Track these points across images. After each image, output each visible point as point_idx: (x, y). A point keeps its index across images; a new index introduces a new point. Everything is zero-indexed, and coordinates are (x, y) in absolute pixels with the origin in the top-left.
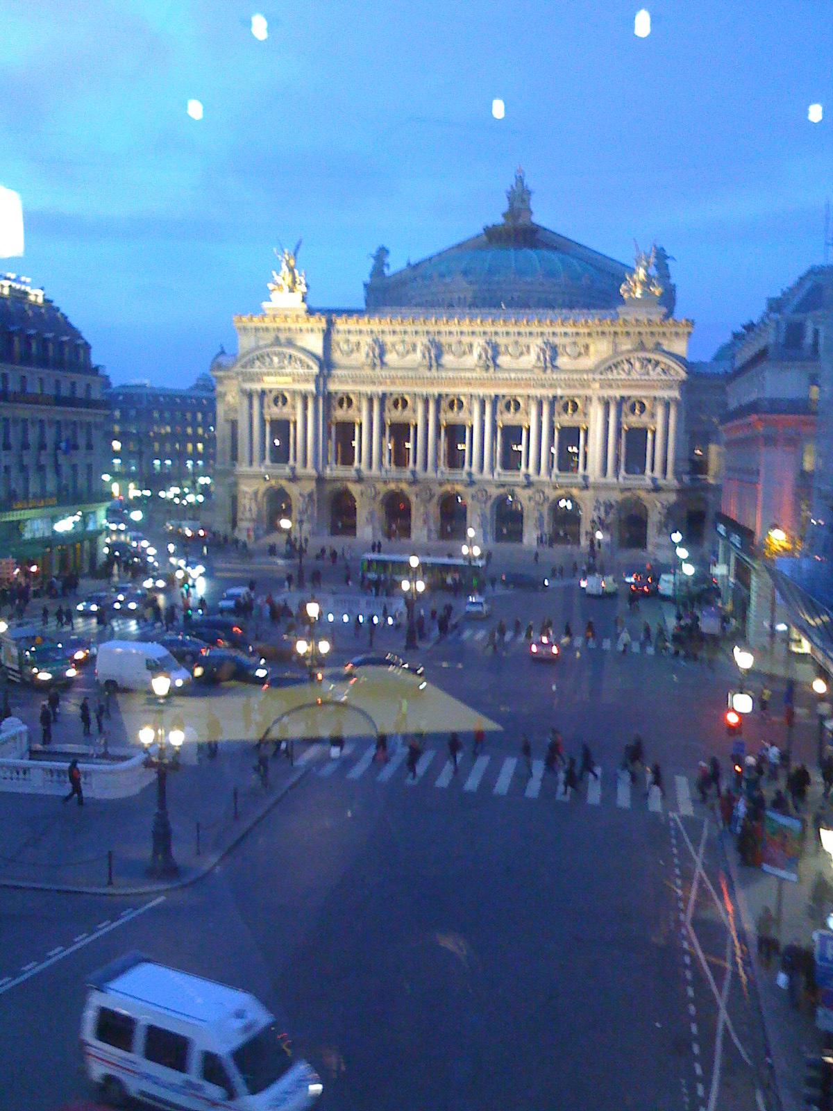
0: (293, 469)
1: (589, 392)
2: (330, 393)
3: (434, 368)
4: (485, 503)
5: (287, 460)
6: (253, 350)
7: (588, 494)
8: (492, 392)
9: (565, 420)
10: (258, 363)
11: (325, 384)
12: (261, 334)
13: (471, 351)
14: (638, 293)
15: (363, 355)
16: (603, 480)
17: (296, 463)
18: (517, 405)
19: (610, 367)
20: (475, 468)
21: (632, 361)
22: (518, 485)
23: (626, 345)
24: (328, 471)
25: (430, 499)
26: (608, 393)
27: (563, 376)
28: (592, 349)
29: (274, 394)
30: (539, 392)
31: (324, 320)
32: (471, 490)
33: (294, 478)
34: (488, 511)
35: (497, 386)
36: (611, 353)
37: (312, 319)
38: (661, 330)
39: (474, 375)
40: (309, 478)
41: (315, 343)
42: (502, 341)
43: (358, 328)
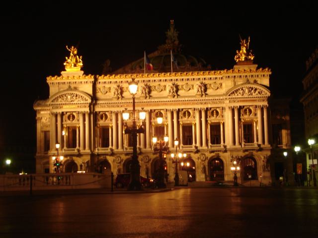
0: (79, 150)
1: (224, 105)
2: (96, 112)
5: (75, 147)
6: (57, 94)
7: (228, 154)
8: (177, 107)
9: (213, 119)
10: (60, 100)
11: (94, 110)
12: (61, 85)
13: (165, 90)
14: (243, 58)
16: (234, 147)
18: (189, 114)
19: (233, 93)
21: (244, 89)
22: (192, 152)
23: (240, 82)
24: (96, 151)
25: (148, 162)
26: (232, 105)
27: (211, 98)
28: (224, 85)
29: (68, 114)
30: (199, 107)
31: (93, 77)
33: (79, 155)
35: (179, 104)
36: (233, 86)
37: (87, 77)
38: (257, 74)
39: (168, 100)
40: (87, 154)
41: (89, 89)
42: (179, 83)
43: (110, 80)
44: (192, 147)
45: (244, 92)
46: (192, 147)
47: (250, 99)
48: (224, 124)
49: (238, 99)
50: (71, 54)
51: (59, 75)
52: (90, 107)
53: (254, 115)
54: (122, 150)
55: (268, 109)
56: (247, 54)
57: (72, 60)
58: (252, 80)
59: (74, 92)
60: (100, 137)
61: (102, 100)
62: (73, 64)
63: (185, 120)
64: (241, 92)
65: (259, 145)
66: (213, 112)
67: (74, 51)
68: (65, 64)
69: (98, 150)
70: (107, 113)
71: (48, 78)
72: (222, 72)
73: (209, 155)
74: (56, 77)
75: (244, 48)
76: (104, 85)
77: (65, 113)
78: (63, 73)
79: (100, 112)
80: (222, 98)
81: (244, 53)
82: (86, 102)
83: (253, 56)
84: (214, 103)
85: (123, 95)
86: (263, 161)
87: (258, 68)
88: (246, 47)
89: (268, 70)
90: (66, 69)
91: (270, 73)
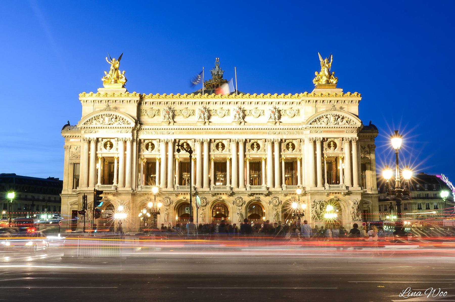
2: (140, 140)
3: (207, 124)
4: (242, 206)
5: (112, 183)
9: (289, 154)
10: (94, 122)
14: (323, 80)
15: (163, 117)
16: (316, 189)
17: (117, 183)
19: (315, 121)
20: (234, 185)
21: (328, 116)
22: (262, 194)
24: (139, 189)
25: (206, 206)
26: (315, 136)
27: (286, 127)
29: (105, 140)
32: (232, 198)
34: (243, 212)
35: (247, 133)
37: (131, 95)
38: (343, 99)
40: (127, 193)
42: (247, 107)
44: (260, 188)
46: (260, 188)
47: (336, 129)
48: (301, 160)
49: (322, 129)
50: (112, 68)
51: (95, 92)
53: (340, 149)
55: (357, 142)
57: (112, 75)
58: (338, 106)
59: (112, 113)
60: (144, 173)
61: (147, 124)
62: (113, 80)
63: (253, 154)
65: (347, 188)
66: (288, 144)
68: (103, 80)
72: (301, 95)
74: (91, 93)
75: (326, 70)
76: (152, 106)
77: (100, 139)
78: (99, 89)
79: (144, 140)
81: (325, 75)
82: (129, 126)
83: (336, 79)
84: (291, 133)
85: (175, 120)
86: (353, 208)
87: (345, 92)
88: (328, 70)
89: (358, 94)
90: (104, 85)
91: (360, 99)
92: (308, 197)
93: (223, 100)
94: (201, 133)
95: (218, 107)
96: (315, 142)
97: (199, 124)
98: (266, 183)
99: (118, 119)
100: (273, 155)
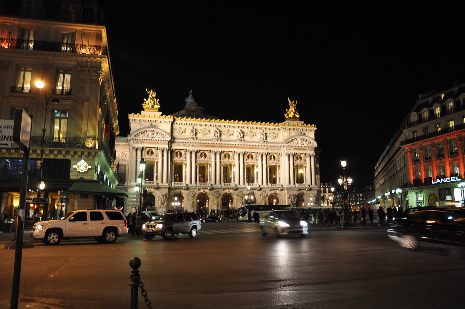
1: (281, 152)
6: (137, 130)
9: (272, 163)
10: (141, 135)
13: (233, 134)
14: (291, 115)
21: (298, 139)
22: (256, 189)
24: (173, 185)
25: (218, 197)
26: (289, 152)
27: (271, 145)
28: (280, 135)
29: (148, 149)
31: (172, 117)
35: (245, 148)
37: (167, 117)
39: (237, 143)
40: (165, 187)
42: (245, 130)
45: (298, 142)
48: (279, 167)
49: (293, 148)
50: (150, 96)
52: (168, 143)
54: (195, 185)
55: (315, 157)
56: (295, 113)
57: (150, 102)
59: (155, 130)
64: (296, 141)
67: (152, 94)
68: (143, 105)
69: (175, 184)
70: (182, 151)
71: (130, 115)
72: (280, 124)
73: (269, 193)
75: (293, 108)
76: (180, 126)
77: (144, 148)
78: (142, 112)
79: (175, 150)
80: (280, 145)
82: (166, 139)
91: (316, 129)
92: (286, 191)
93: (230, 125)
94: (215, 147)
95: (226, 129)
96: (289, 156)
97: (214, 140)
98: (257, 181)
99: (158, 134)
100: (262, 163)
